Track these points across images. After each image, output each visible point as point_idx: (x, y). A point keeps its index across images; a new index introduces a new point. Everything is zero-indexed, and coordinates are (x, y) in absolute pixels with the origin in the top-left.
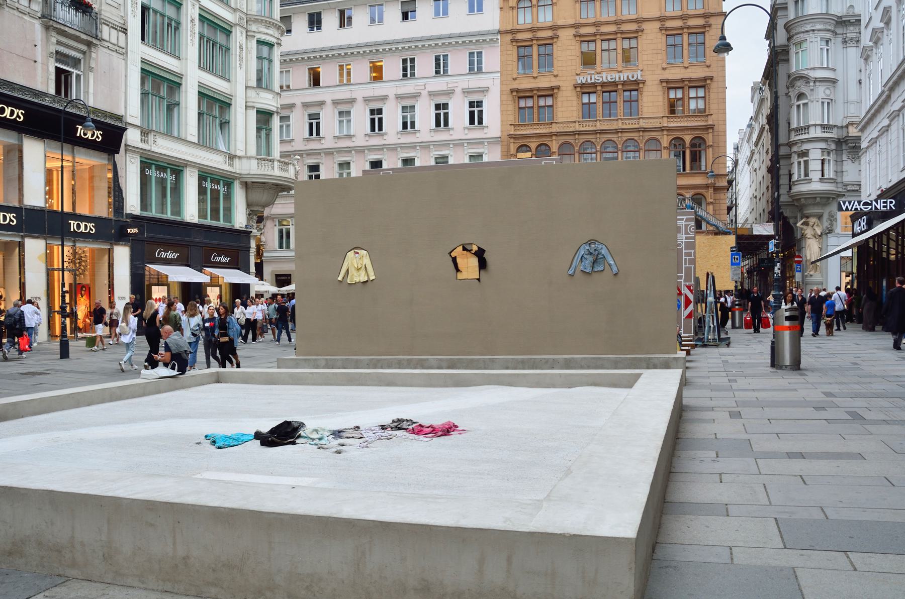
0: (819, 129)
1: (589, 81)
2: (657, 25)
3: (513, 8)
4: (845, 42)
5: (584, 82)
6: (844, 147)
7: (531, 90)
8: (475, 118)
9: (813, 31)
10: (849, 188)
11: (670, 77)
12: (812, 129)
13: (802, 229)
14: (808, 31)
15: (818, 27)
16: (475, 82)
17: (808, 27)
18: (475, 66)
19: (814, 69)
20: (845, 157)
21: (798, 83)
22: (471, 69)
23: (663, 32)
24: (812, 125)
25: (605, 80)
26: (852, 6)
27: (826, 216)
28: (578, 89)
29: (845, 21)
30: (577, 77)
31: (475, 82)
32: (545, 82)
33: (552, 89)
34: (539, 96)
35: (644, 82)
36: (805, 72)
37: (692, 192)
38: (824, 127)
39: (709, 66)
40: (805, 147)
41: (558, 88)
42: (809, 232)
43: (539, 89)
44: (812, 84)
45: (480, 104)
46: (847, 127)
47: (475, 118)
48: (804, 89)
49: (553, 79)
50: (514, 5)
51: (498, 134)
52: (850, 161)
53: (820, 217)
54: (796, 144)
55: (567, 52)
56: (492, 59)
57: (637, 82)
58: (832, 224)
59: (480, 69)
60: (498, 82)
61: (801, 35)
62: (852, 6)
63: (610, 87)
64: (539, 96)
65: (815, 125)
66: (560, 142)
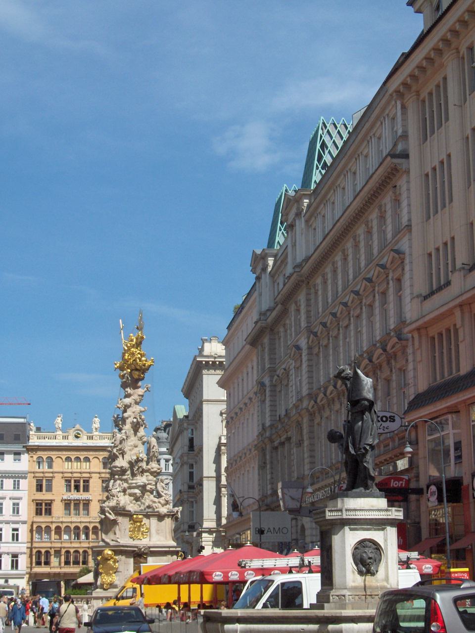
1: (68, 498)
2: (98, 475)
5: (66, 498)
8: (16, 510)
16: (16, 494)
18: (16, 486)
22: (14, 488)
31: (16, 494)
35: (91, 500)
41: (54, 500)
45: (18, 504)
47: (16, 510)
51: (26, 520)
55: (59, 485)
56: (23, 483)
57: (89, 500)
59: (18, 488)
60: (27, 495)
63: (77, 503)
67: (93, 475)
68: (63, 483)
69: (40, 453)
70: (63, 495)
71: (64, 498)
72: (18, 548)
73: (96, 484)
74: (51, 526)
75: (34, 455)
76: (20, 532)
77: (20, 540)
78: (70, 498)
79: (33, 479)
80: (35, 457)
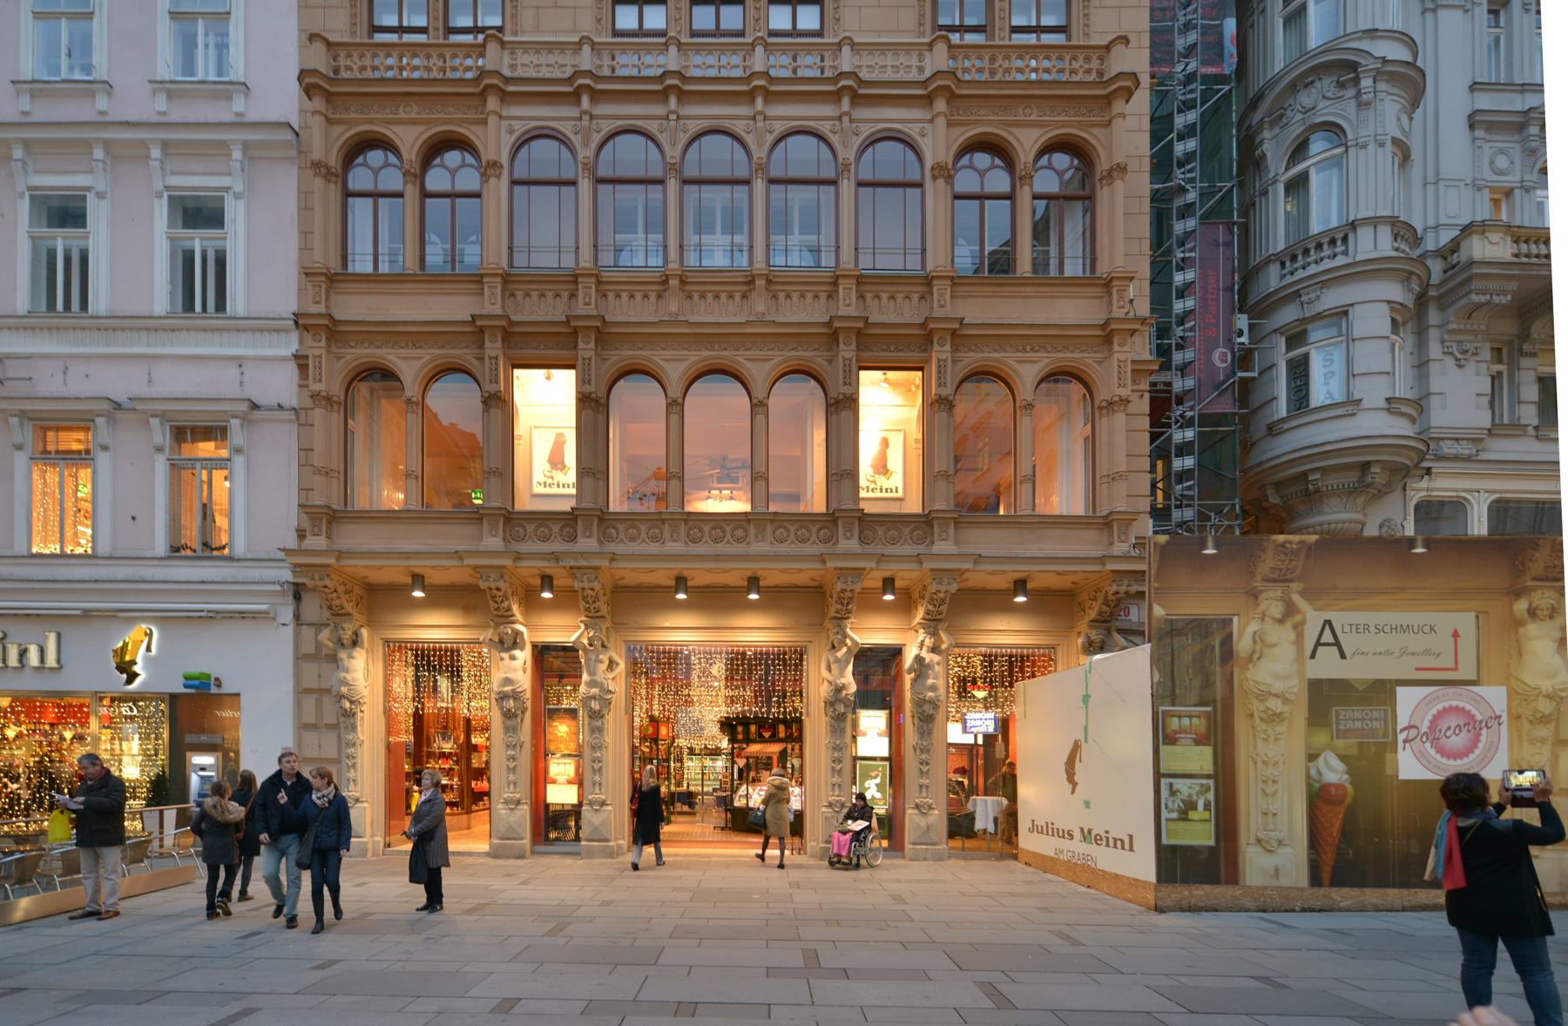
0: (1385, 233)
12: (1364, 237)
24: (1366, 221)
40: (1332, 299)
65: (1375, 221)
72: (232, 372)
76: (237, 237)
77: (237, 301)
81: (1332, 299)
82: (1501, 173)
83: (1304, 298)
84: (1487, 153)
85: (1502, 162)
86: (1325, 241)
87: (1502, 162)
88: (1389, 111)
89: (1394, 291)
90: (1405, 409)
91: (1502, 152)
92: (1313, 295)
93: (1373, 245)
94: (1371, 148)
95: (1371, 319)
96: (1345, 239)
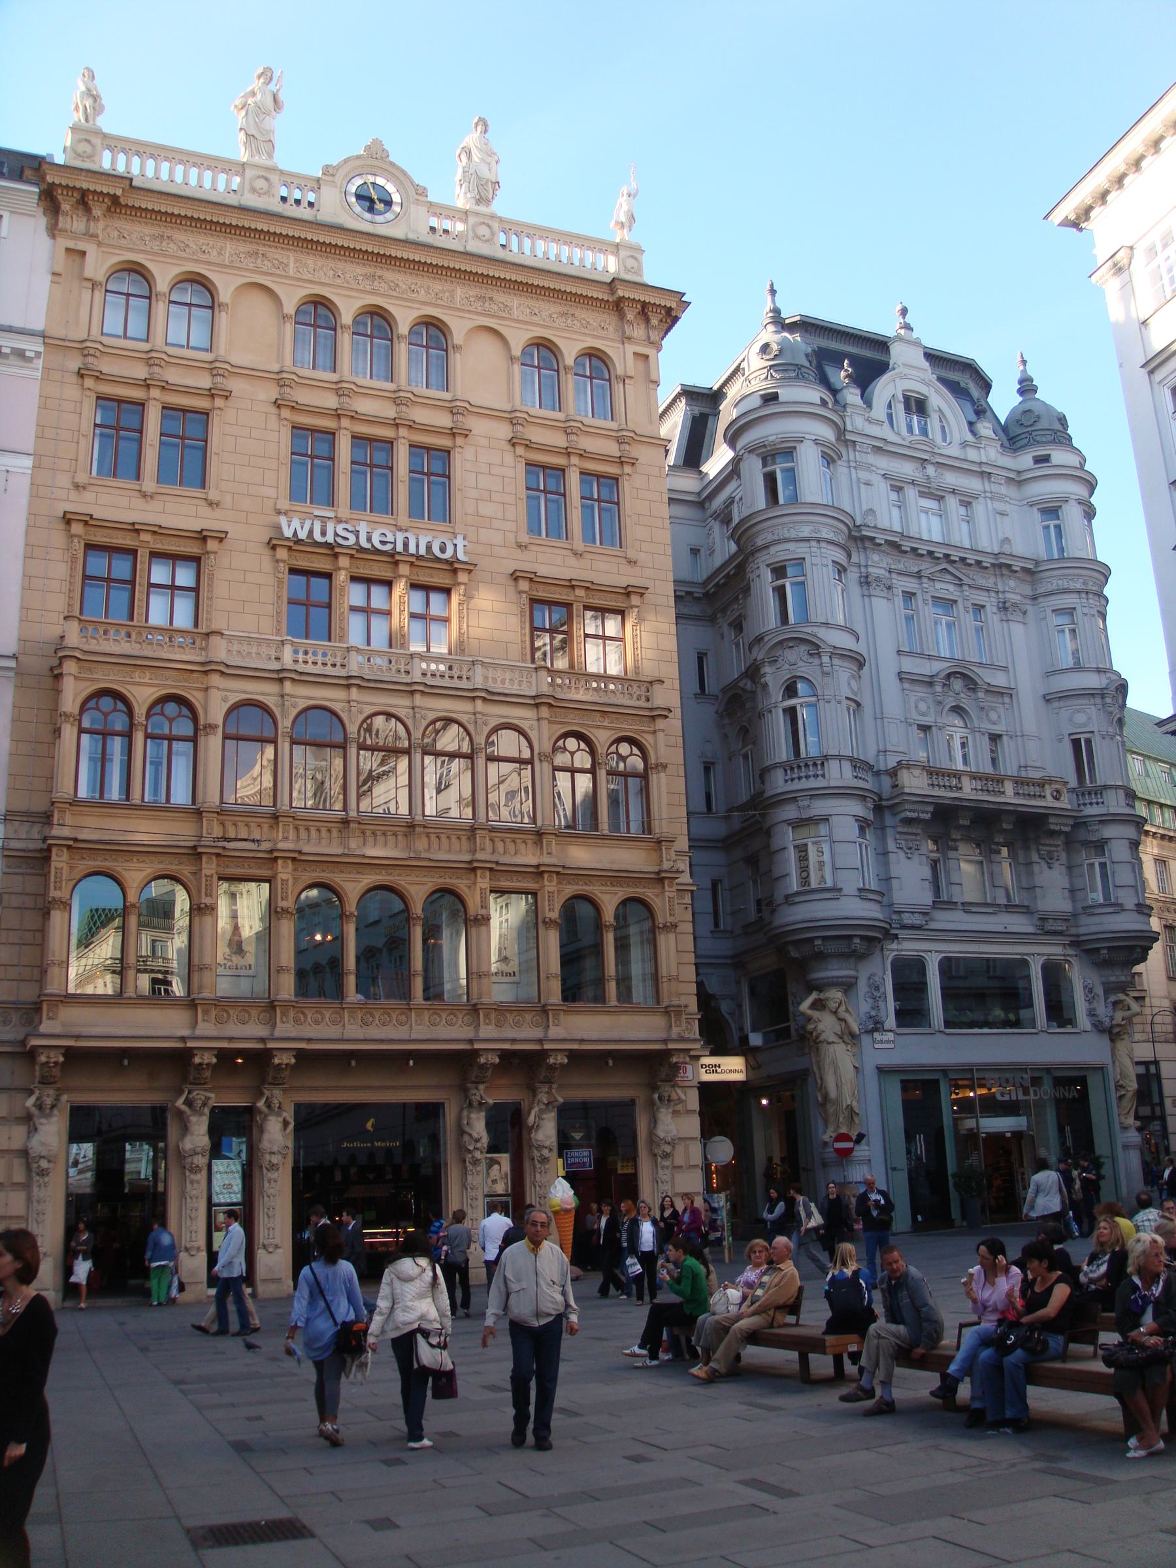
0: (847, 766)
1: (317, 537)
2: (504, 431)
3: (94, 285)
4: (865, 582)
5: (303, 535)
6: (889, 820)
7: (135, 529)
9: (818, 541)
10: (908, 919)
11: (543, 571)
12: (833, 767)
13: (809, 1019)
14: (807, 540)
15: (826, 533)
17: (805, 532)
19: (826, 624)
20: (891, 846)
21: (791, 655)
23: (520, 450)
24: (834, 757)
25: (364, 543)
26: (871, 511)
27: (862, 987)
28: (282, 554)
29: (863, 539)
30: (283, 520)
32: (179, 512)
33: (202, 537)
34: (154, 555)
36: (808, 630)
37: (622, 893)
38: (858, 764)
39: (632, 562)
40: (819, 808)
42: (826, 1025)
43: (158, 531)
44: (826, 659)
46: (893, 773)
48: (803, 670)
49: (205, 511)
50: (100, 276)
52: (902, 855)
53: (848, 986)
54: (795, 799)
57: (453, 567)
58: (876, 1007)
61: (791, 546)
62: (871, 511)
64: (154, 555)
65: (840, 758)
66: (234, 698)
67: (472, 423)
68: (277, 440)
69: (135, 240)
70: (279, 513)
71: (288, 533)
73: (487, 477)
74: (195, 697)
75: (91, 249)
78: (330, 538)
79: (72, 391)
80: (97, 264)
81: (819, 808)
82: (923, 714)
83: (800, 804)
84: (913, 699)
85: (923, 706)
86: (810, 763)
87: (923, 706)
88: (844, 673)
89: (857, 808)
90: (871, 896)
91: (922, 699)
92: (806, 803)
93: (839, 774)
94: (833, 703)
95: (845, 828)
96: (822, 764)
